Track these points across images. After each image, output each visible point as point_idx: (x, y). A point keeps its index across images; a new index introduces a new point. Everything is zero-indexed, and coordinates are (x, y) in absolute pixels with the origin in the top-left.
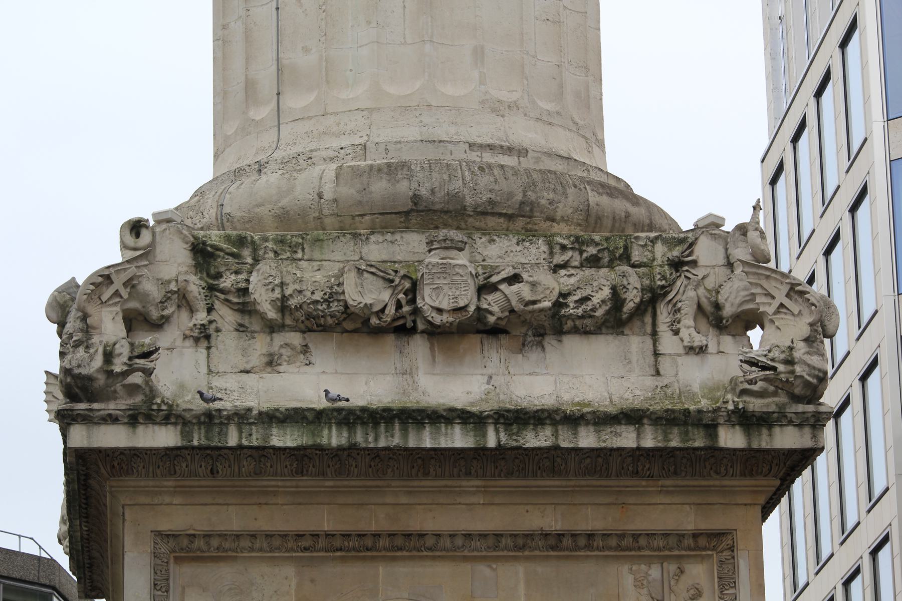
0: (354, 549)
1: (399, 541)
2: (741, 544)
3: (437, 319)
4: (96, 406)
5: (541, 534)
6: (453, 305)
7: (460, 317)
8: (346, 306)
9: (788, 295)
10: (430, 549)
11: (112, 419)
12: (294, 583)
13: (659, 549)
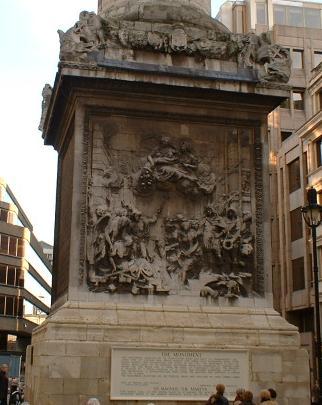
11: (76, 67)
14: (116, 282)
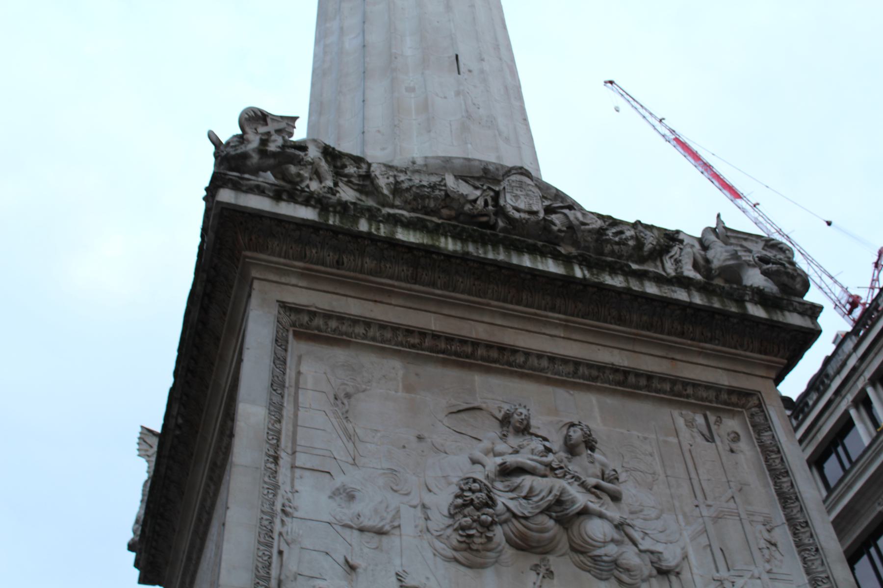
0: (456, 354)
1: (494, 354)
2: (767, 402)
3: (517, 215)
4: (247, 176)
5: (611, 368)
6: (527, 208)
7: (533, 218)
8: (447, 195)
9: (763, 249)
12: (401, 373)
13: (702, 399)
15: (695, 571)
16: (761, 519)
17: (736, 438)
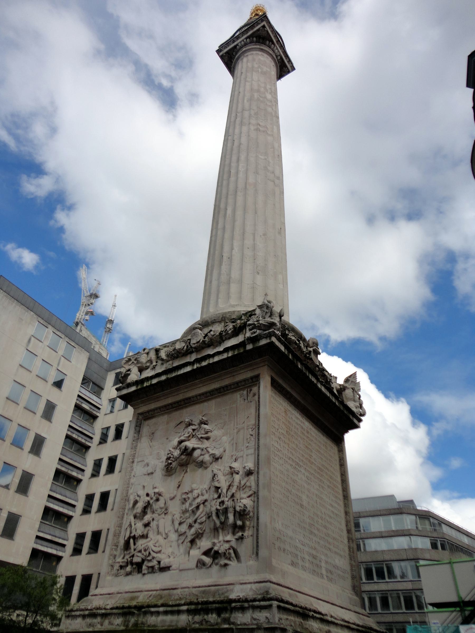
3: (193, 346)
7: (198, 344)
10: (193, 402)
14: (132, 563)
15: (226, 455)
16: (251, 427)
17: (254, 395)
